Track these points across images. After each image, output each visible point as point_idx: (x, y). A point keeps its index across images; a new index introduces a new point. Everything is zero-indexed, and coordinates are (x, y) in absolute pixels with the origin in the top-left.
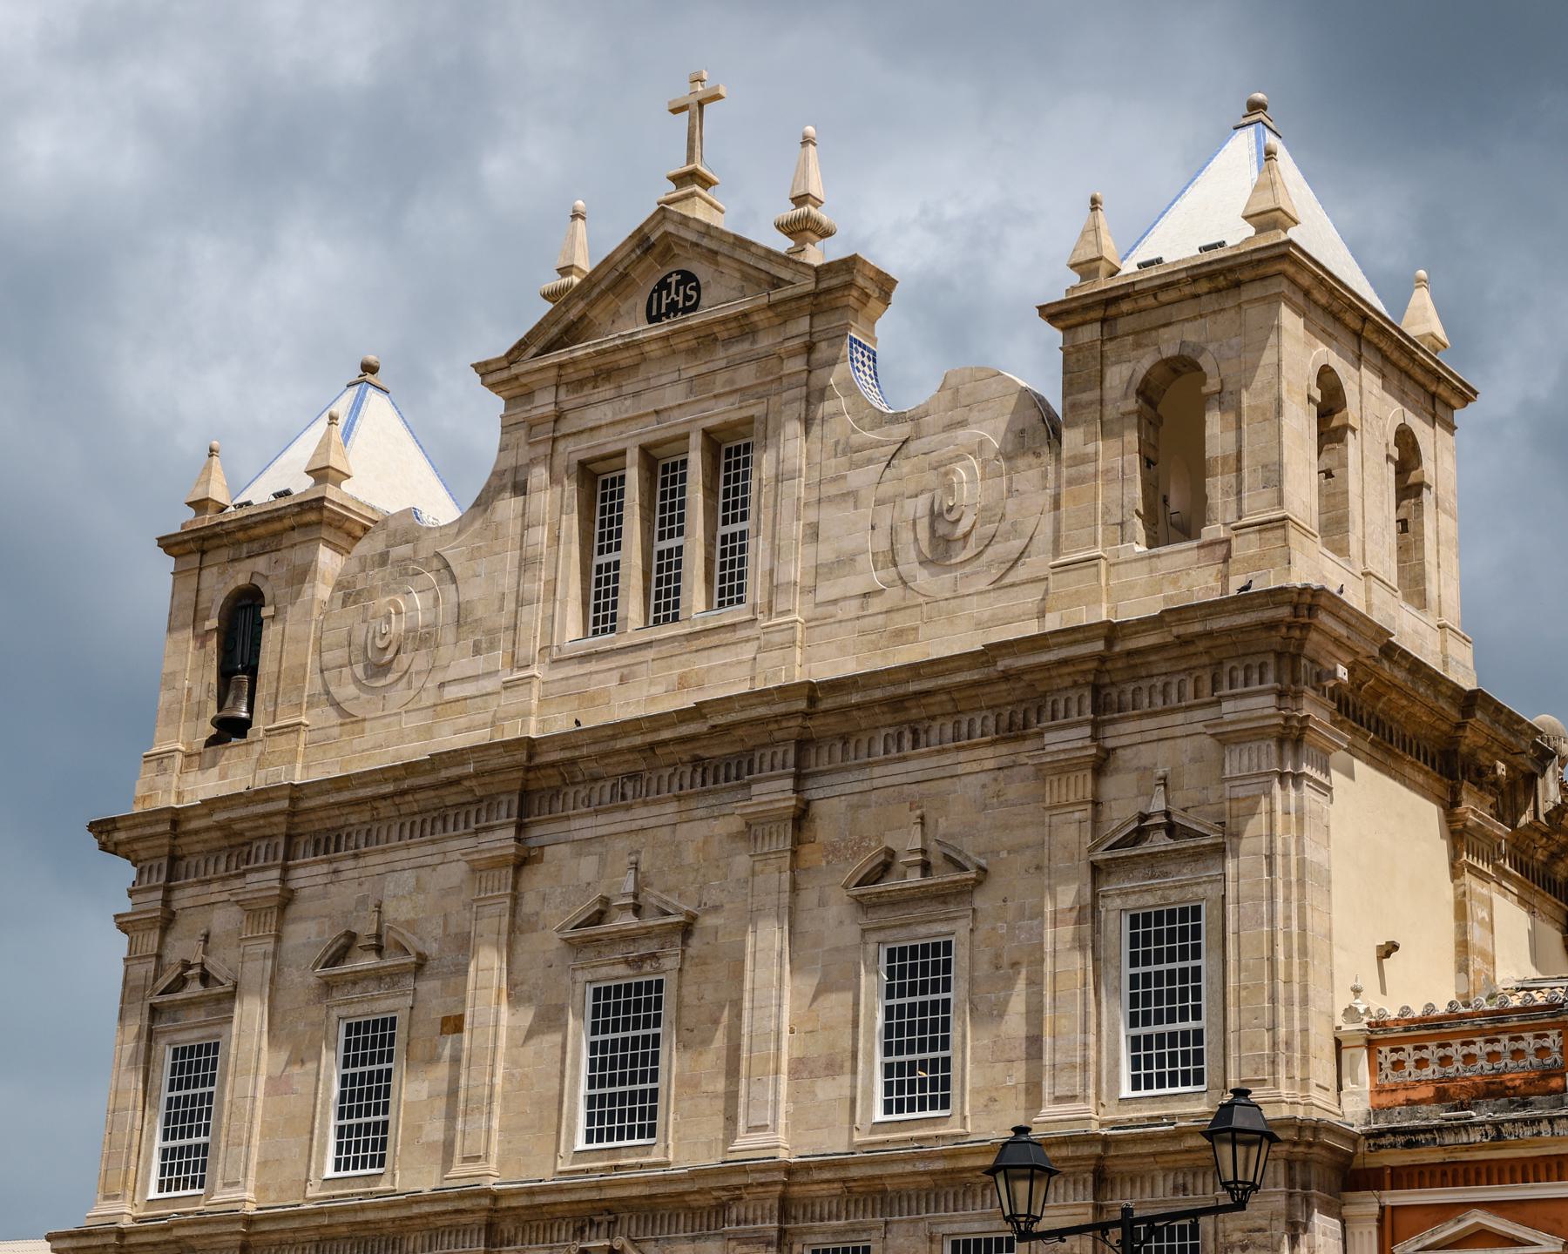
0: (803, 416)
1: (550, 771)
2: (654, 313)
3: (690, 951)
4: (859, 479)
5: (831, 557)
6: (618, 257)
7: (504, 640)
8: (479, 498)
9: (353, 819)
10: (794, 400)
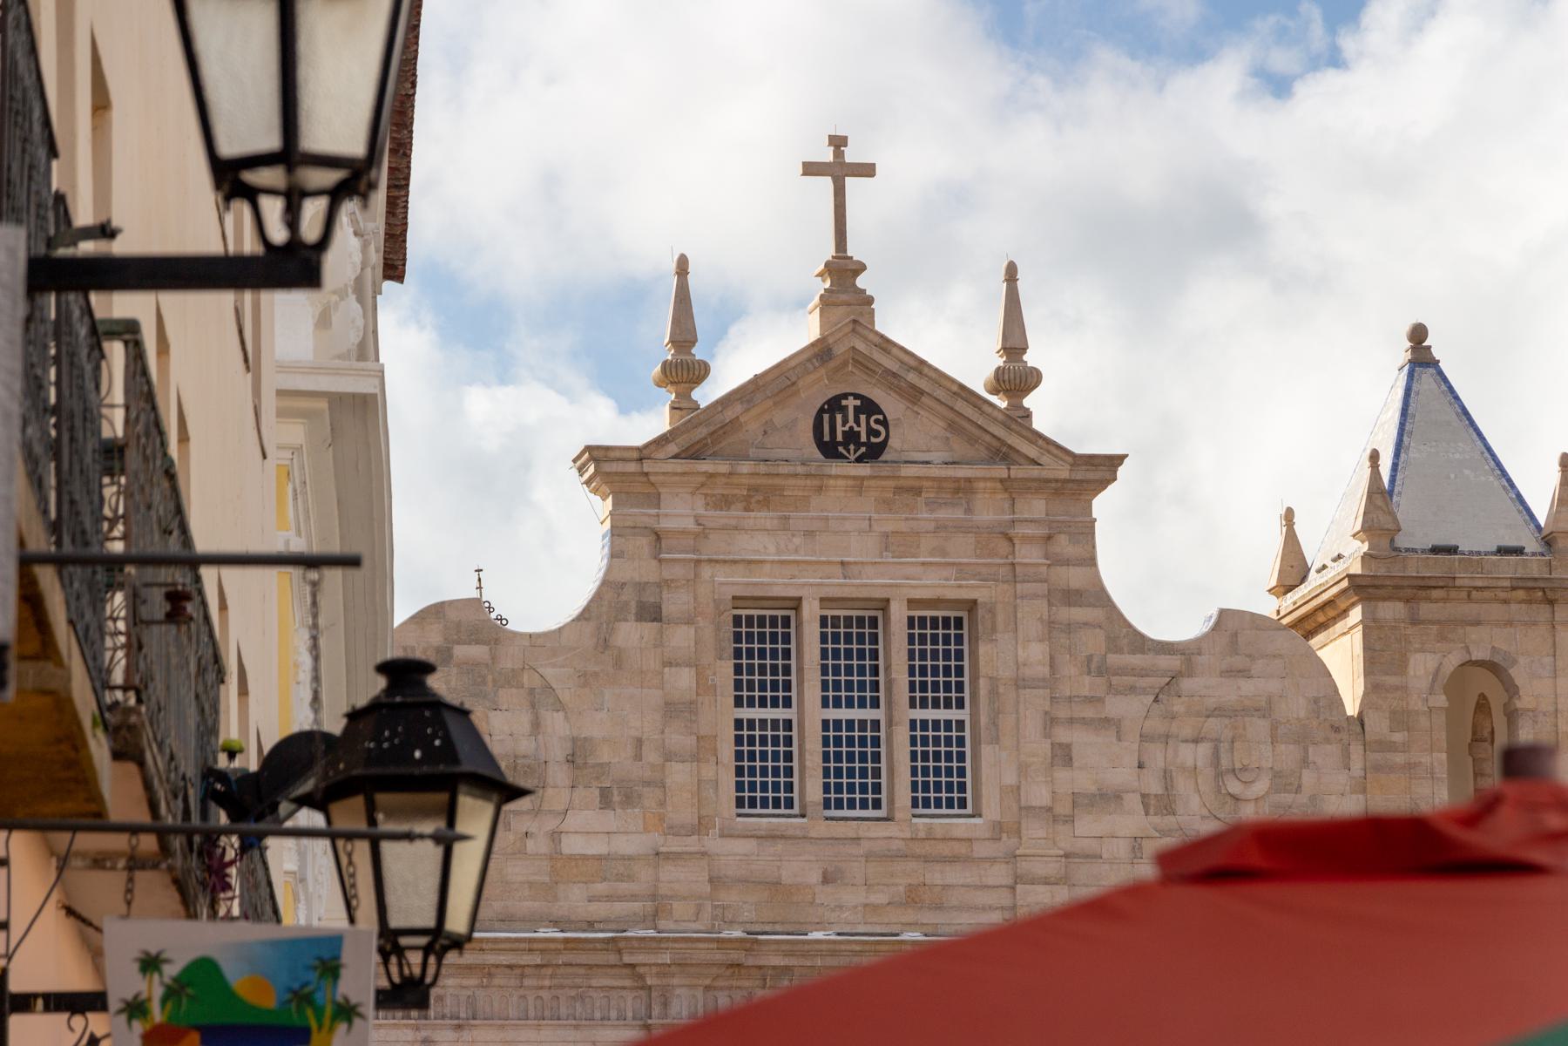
0: (1045, 617)
2: (827, 438)
4: (1128, 708)
5: (1093, 789)
7: (650, 797)
8: (587, 610)
10: (1035, 596)
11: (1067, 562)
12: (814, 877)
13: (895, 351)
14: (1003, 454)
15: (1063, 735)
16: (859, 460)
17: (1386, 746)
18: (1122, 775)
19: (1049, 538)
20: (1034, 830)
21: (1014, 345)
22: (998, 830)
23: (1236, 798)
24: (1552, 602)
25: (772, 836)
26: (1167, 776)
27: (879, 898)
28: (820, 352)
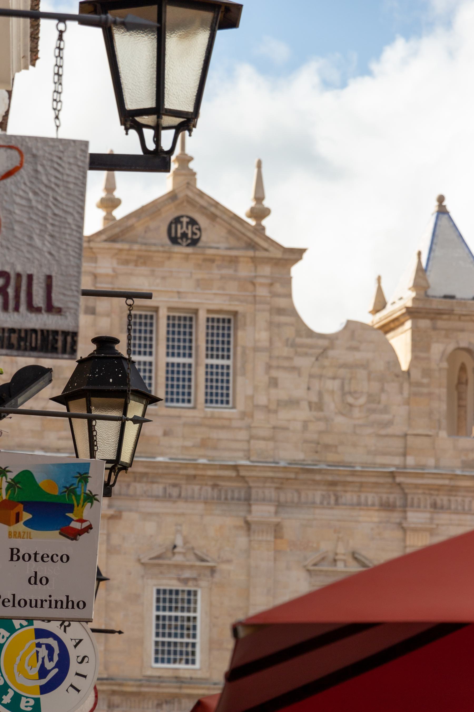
11: (279, 295)
14: (252, 246)
15: (274, 373)
16: (188, 245)
18: (300, 393)
19: (271, 285)
20: (260, 416)
21: (259, 198)
22: (244, 415)
23: (351, 405)
26: (320, 394)
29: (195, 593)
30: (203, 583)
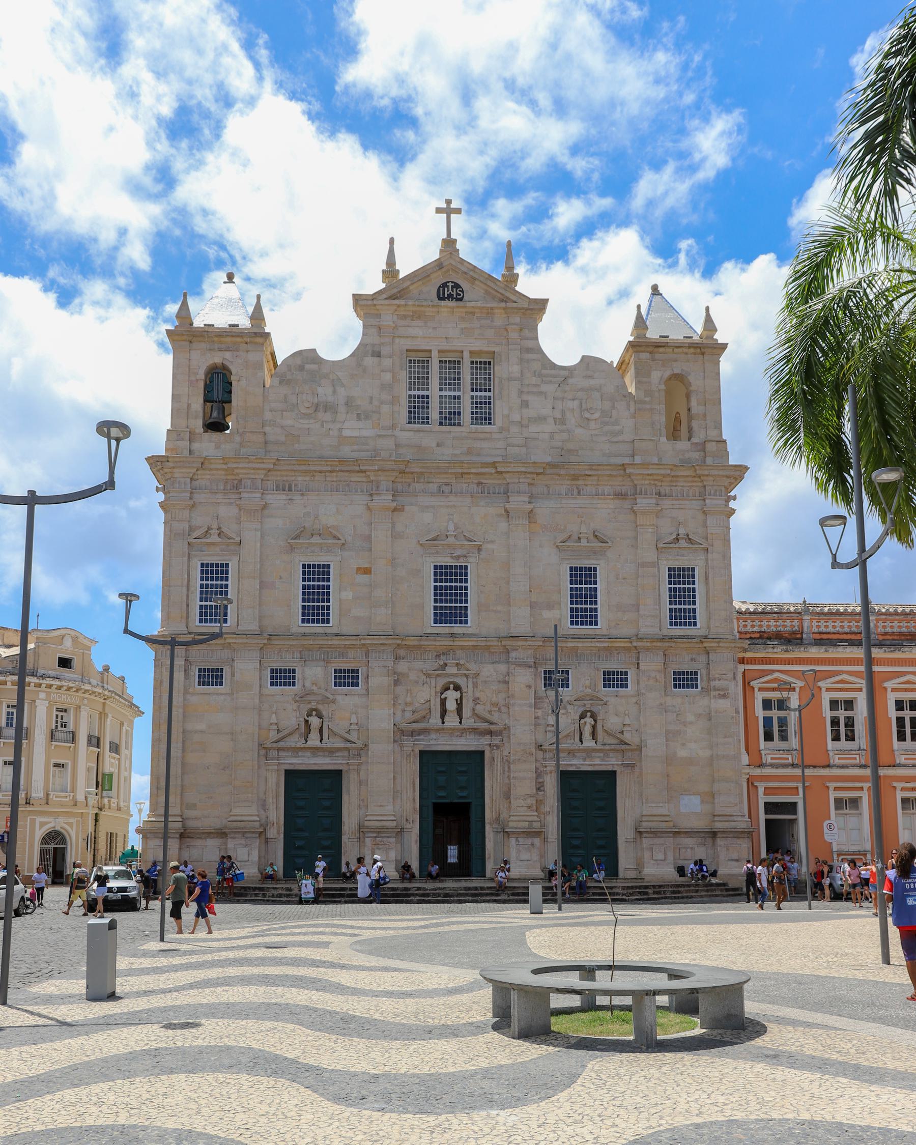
1: (410, 475)
3: (481, 556)
6: (429, 267)
9: (300, 479)
12: (434, 445)
13: (465, 264)
15: (525, 397)
17: (642, 402)
19: (521, 330)
20: (515, 429)
22: (501, 430)
23: (588, 419)
24: (703, 354)
25: (418, 431)
26: (563, 412)
27: (457, 452)
28: (438, 265)
29: (466, 568)
30: (471, 559)
